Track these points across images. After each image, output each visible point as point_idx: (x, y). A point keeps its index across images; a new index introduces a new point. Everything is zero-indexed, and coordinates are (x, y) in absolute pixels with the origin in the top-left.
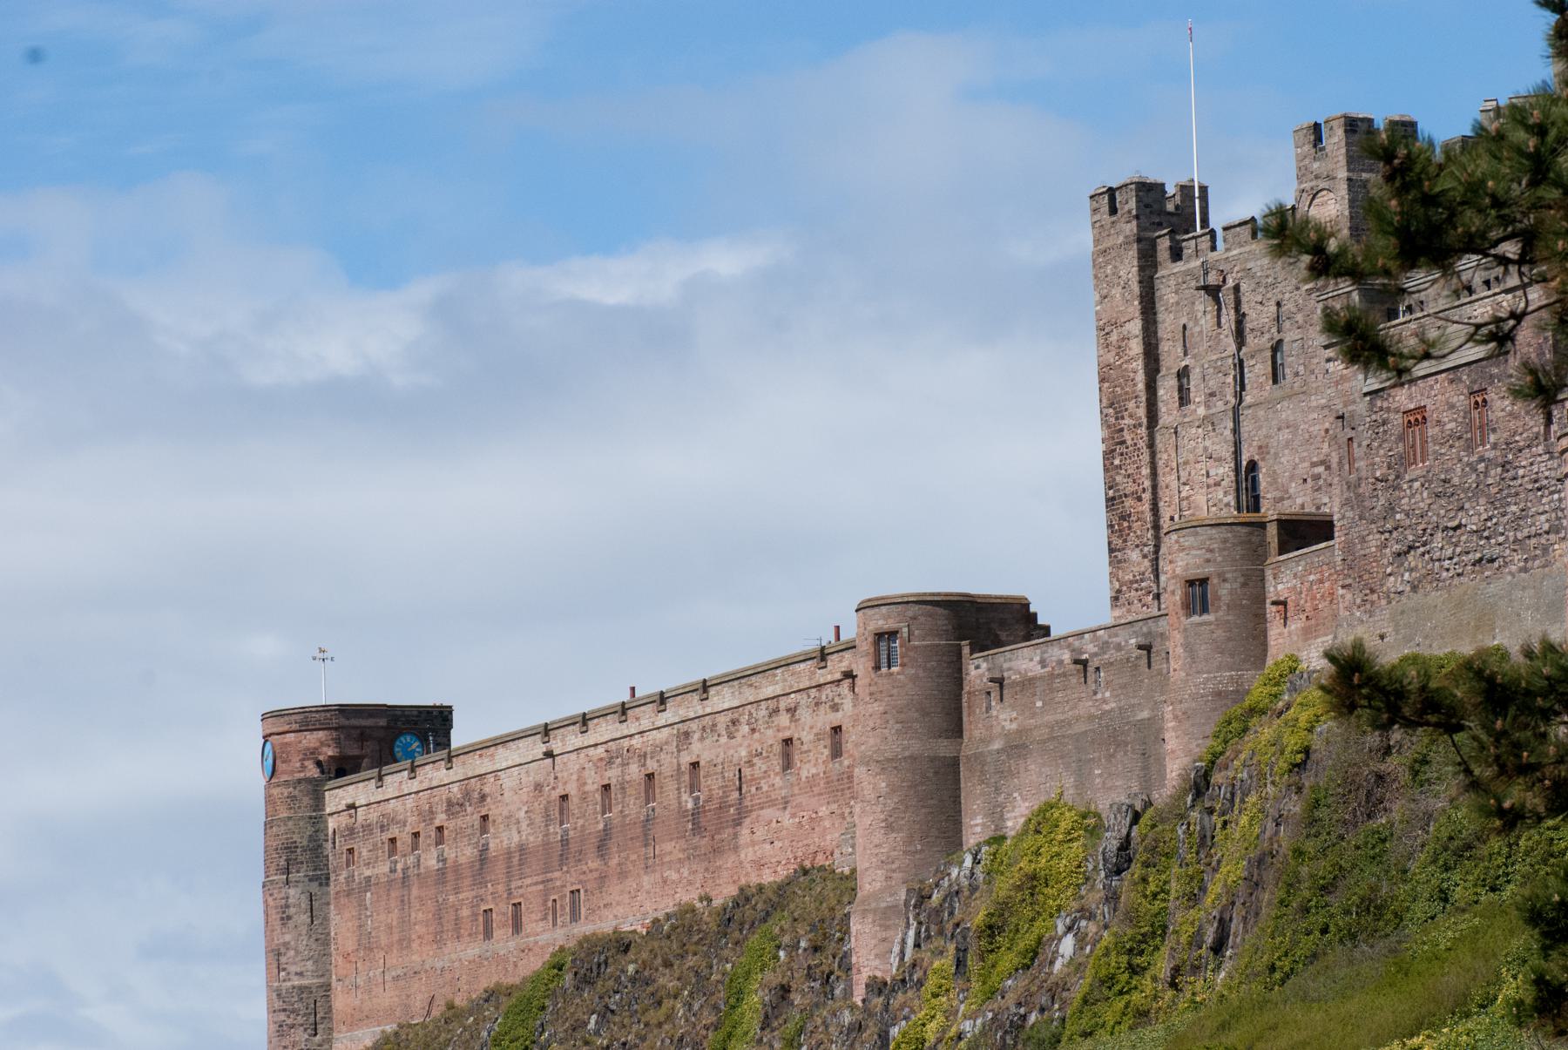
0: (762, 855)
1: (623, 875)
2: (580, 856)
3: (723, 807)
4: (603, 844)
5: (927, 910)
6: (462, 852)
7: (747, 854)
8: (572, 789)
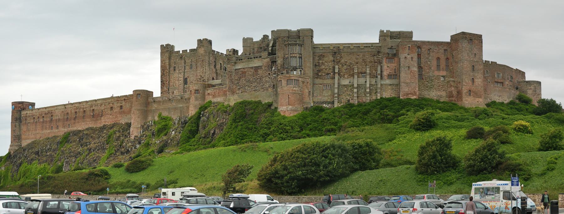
0: (107, 120)
1: (78, 122)
2: (70, 120)
3: (99, 115)
4: (75, 119)
5: (145, 128)
6: (48, 119)
7: (103, 121)
8: (69, 112)
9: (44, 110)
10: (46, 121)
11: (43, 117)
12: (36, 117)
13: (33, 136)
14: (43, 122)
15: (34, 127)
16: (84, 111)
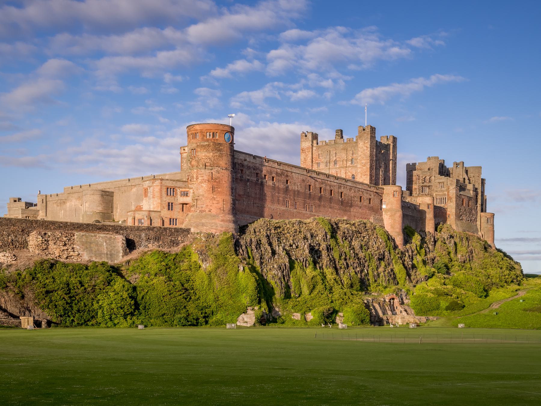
1: (324, 207)
3: (348, 203)
4: (320, 198)
9: (276, 165)
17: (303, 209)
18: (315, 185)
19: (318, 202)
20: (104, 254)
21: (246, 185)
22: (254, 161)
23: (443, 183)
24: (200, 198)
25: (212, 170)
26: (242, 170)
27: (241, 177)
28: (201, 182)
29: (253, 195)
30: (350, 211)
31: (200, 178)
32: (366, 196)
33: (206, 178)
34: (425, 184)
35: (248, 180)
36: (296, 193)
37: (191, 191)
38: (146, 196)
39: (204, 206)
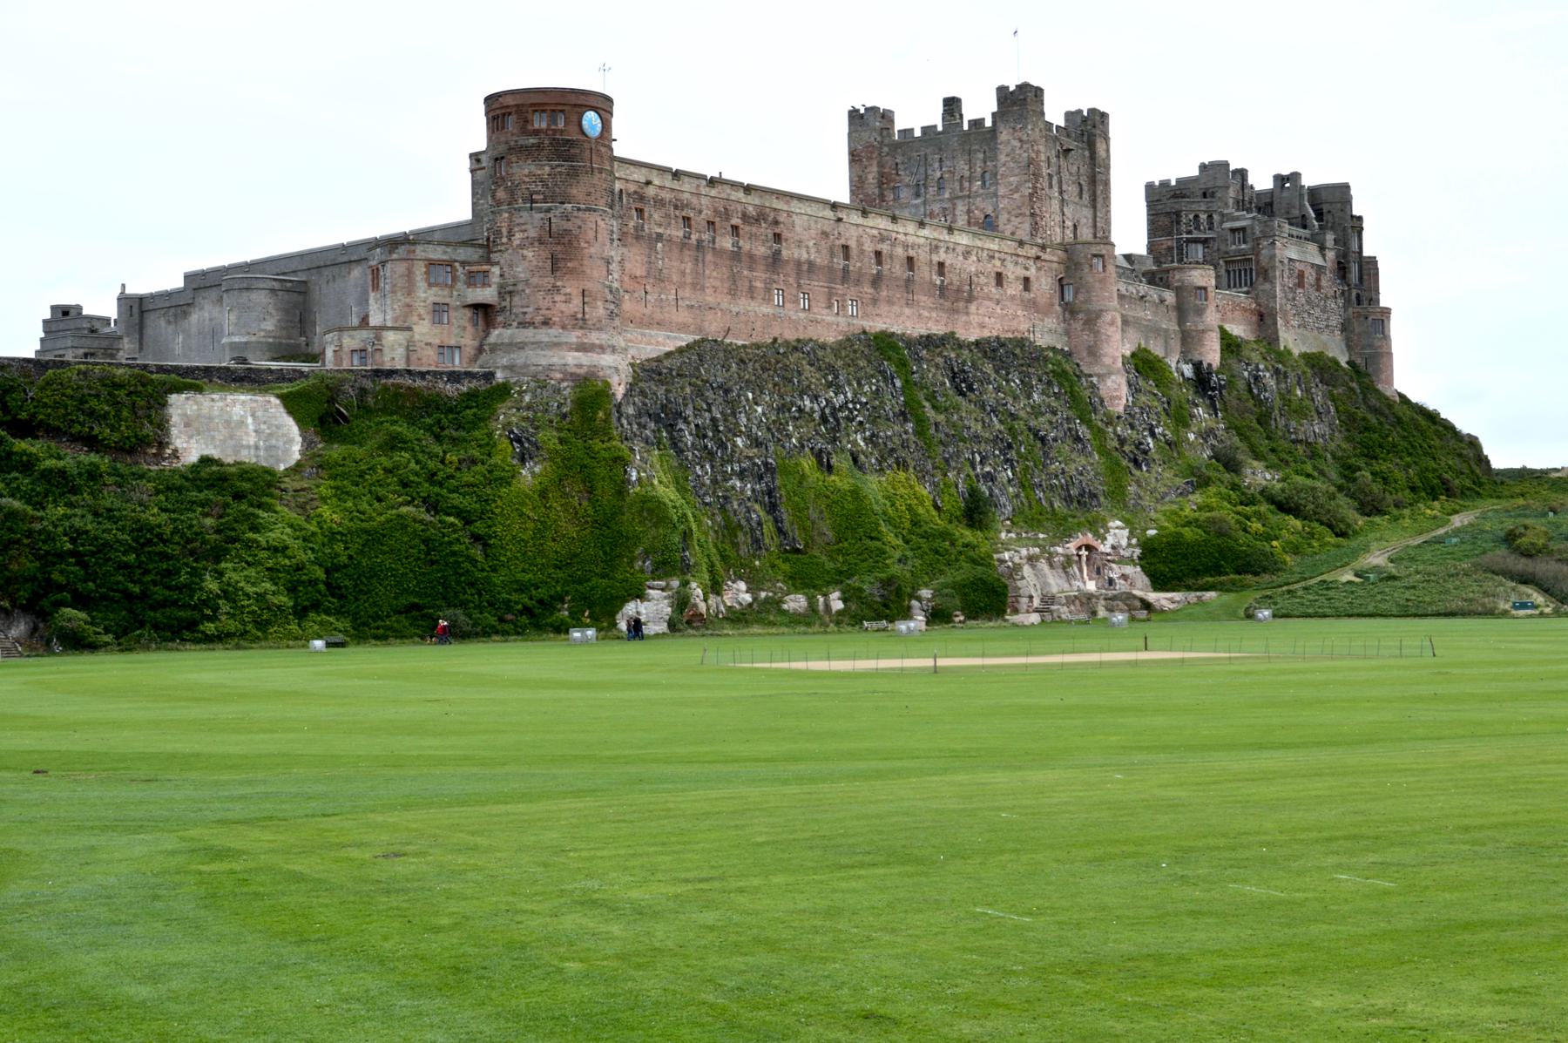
1: (890, 302)
3: (959, 290)
4: (876, 281)
7: (975, 319)
8: (853, 244)
9: (741, 195)
10: (751, 257)
11: (735, 228)
12: (699, 221)
13: (683, 316)
14: (736, 256)
15: (689, 267)
16: (910, 260)
17: (825, 311)
18: (860, 244)
19: (871, 290)
20: (249, 447)
21: (653, 248)
22: (675, 185)
23: (1243, 229)
24: (520, 287)
25: (548, 210)
26: (640, 211)
27: (636, 228)
28: (521, 246)
29: (675, 278)
30: (967, 314)
31: (518, 235)
32: (1013, 272)
33: (533, 233)
34: (1195, 235)
35: (659, 237)
36: (805, 267)
37: (496, 270)
38: (376, 287)
39: (530, 310)
